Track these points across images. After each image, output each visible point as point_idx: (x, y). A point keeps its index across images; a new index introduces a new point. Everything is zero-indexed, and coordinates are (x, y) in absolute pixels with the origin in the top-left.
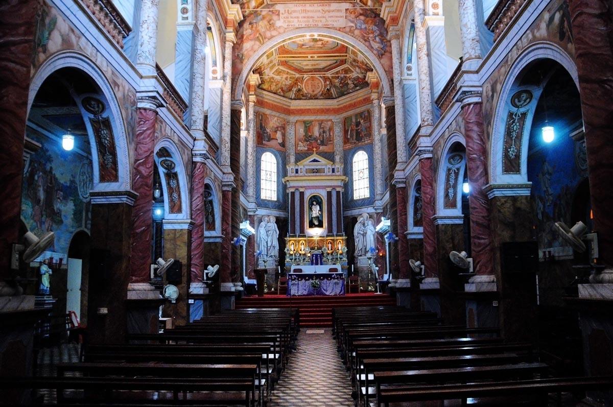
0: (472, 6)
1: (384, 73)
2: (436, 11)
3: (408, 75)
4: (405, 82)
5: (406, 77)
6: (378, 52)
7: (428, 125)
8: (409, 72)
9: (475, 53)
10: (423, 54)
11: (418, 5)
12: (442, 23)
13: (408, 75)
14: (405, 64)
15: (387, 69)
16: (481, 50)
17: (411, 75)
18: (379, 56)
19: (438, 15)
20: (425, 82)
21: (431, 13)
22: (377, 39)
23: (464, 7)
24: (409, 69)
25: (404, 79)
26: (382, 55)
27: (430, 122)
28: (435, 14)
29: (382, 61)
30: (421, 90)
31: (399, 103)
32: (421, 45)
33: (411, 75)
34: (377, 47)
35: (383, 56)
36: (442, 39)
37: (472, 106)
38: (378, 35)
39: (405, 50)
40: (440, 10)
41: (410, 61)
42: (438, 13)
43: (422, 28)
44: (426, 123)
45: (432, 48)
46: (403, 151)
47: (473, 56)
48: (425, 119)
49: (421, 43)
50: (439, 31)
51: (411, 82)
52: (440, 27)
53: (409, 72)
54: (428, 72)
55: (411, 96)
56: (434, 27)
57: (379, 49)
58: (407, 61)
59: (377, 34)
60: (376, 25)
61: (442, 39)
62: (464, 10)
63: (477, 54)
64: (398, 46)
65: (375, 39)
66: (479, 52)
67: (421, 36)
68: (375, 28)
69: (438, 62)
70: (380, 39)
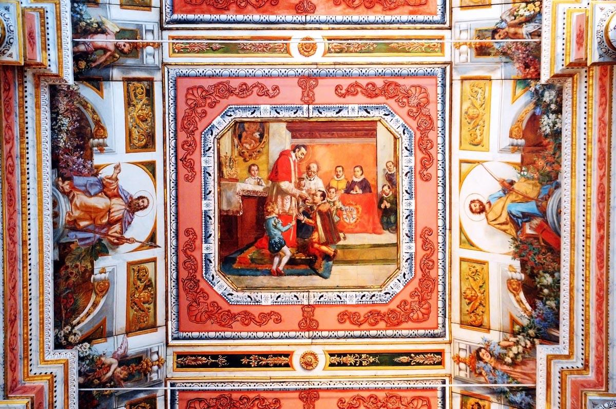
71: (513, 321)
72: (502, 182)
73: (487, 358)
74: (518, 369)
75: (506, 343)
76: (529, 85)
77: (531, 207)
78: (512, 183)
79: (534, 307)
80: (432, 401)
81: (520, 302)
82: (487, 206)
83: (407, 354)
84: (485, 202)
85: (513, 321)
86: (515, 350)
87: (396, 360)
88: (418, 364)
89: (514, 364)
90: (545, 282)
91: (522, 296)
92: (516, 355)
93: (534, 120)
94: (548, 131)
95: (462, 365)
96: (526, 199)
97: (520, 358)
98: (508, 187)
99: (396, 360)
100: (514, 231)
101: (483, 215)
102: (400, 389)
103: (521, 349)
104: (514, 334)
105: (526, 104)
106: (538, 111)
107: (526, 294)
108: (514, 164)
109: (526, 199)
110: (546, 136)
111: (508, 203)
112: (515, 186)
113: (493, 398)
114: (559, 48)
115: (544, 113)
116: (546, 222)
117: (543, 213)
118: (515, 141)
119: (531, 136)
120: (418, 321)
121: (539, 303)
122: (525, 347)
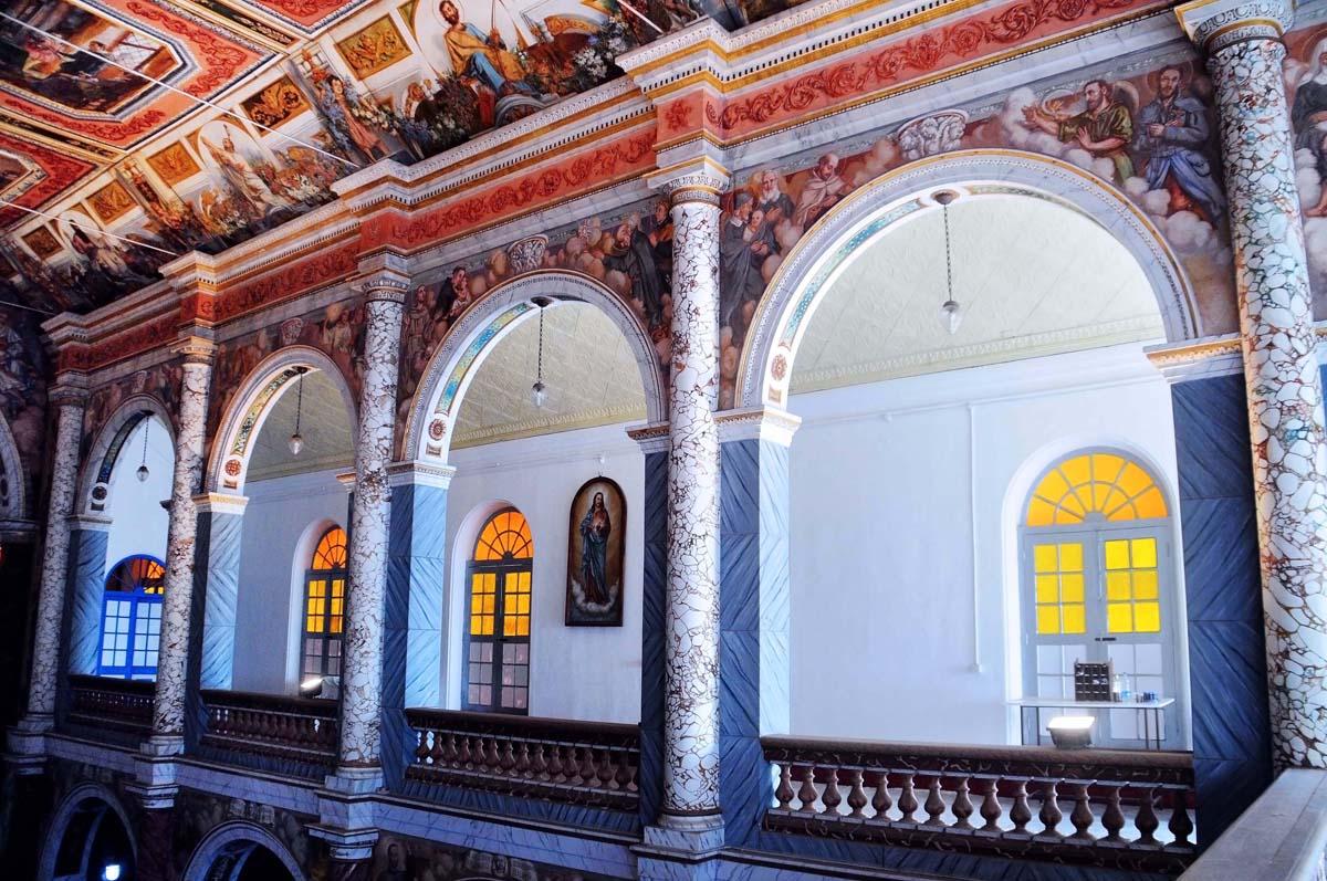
0: (377, 650)
1: (17, 458)
2: (232, 479)
3: (94, 507)
4: (84, 526)
5: (89, 512)
6: (10, 401)
7: (173, 733)
8: (97, 502)
9: (372, 753)
10: (183, 563)
11: (189, 444)
12: (240, 510)
13: (94, 507)
14: (93, 483)
15: (25, 448)
16: (382, 745)
17: (101, 508)
18: (10, 411)
19: (235, 488)
20: (180, 632)
21: (221, 482)
22: (14, 366)
23: (363, 650)
24: (100, 494)
25: (83, 520)
26: (20, 409)
27: (178, 725)
28: (230, 486)
29: (18, 426)
30: (165, 649)
31: (56, 567)
32: (182, 542)
33: (101, 508)
34: (9, 387)
35: (22, 414)
36: (234, 546)
37: (354, 866)
38: (17, 358)
39: (100, 452)
40: (240, 479)
41: (105, 476)
42: (236, 484)
43: (190, 503)
44: (168, 729)
45: (210, 565)
46: (48, 686)
47: (367, 761)
48: (167, 719)
49: (181, 538)
50: (230, 527)
51: (98, 527)
52: (233, 516)
53: (97, 502)
54: (189, 609)
55: (92, 563)
56: (222, 515)
57: (13, 393)
58: (100, 476)
59: (14, 353)
60: (16, 329)
61: (234, 546)
62: (362, 655)
63: (374, 757)
64: (78, 426)
65: (9, 365)
66: (377, 750)
67: (186, 522)
68: (14, 337)
69: (217, 598)
70: (22, 368)
71: (389, 102)
72: (495, 34)
73: (338, 89)
74: (358, 125)
75: (366, 104)
76: (614, 13)
77: (498, 80)
78: (503, 46)
79: (417, 118)
80: (248, 59)
81: (409, 104)
82: (459, 26)
83: (255, 22)
84: (461, 20)
85: (389, 102)
86: (369, 115)
87: (235, 17)
88: (258, 31)
89: (359, 119)
90: (446, 122)
91: (415, 104)
92: (365, 118)
93: (580, 41)
94: (582, 63)
95: (309, 68)
96: (500, 70)
97: (368, 123)
98: (494, 43)
99: (235, 17)
100: (460, 71)
101: (448, 25)
102: (220, 35)
103: (375, 120)
104: (380, 107)
105: (590, 21)
106: (594, 40)
107: (419, 106)
108: (521, 40)
109: (500, 70)
110: (575, 64)
111: (482, 51)
112: (502, 52)
113: (314, 108)
114: (662, 75)
115: (596, 49)
116: (496, 101)
117: (502, 93)
118: (545, 29)
119: (562, 45)
120: (292, 12)
121: (424, 124)
122: (380, 124)
